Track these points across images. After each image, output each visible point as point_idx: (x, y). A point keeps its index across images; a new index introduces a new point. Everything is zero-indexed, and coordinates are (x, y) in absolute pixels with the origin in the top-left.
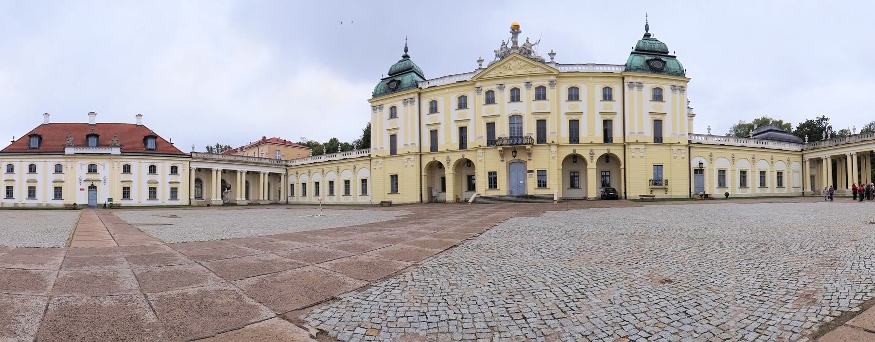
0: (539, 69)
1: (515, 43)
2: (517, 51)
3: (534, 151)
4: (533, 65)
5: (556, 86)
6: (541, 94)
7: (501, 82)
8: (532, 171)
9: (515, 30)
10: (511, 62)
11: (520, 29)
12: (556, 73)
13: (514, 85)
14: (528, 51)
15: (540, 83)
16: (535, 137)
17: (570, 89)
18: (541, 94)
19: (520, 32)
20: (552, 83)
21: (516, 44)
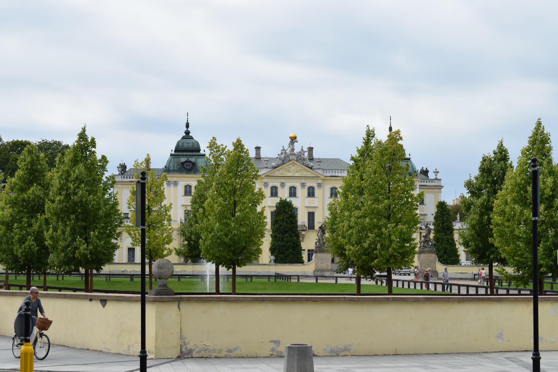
0: (309, 173)
1: (293, 150)
2: (294, 158)
3: (306, 235)
4: (307, 170)
5: (322, 187)
6: (311, 193)
7: (283, 181)
8: (304, 250)
9: (293, 139)
10: (290, 166)
11: (298, 139)
12: (322, 177)
13: (292, 184)
14: (303, 158)
15: (311, 184)
16: (307, 225)
17: (332, 189)
18: (311, 193)
19: (297, 142)
20: (319, 185)
21: (293, 151)
